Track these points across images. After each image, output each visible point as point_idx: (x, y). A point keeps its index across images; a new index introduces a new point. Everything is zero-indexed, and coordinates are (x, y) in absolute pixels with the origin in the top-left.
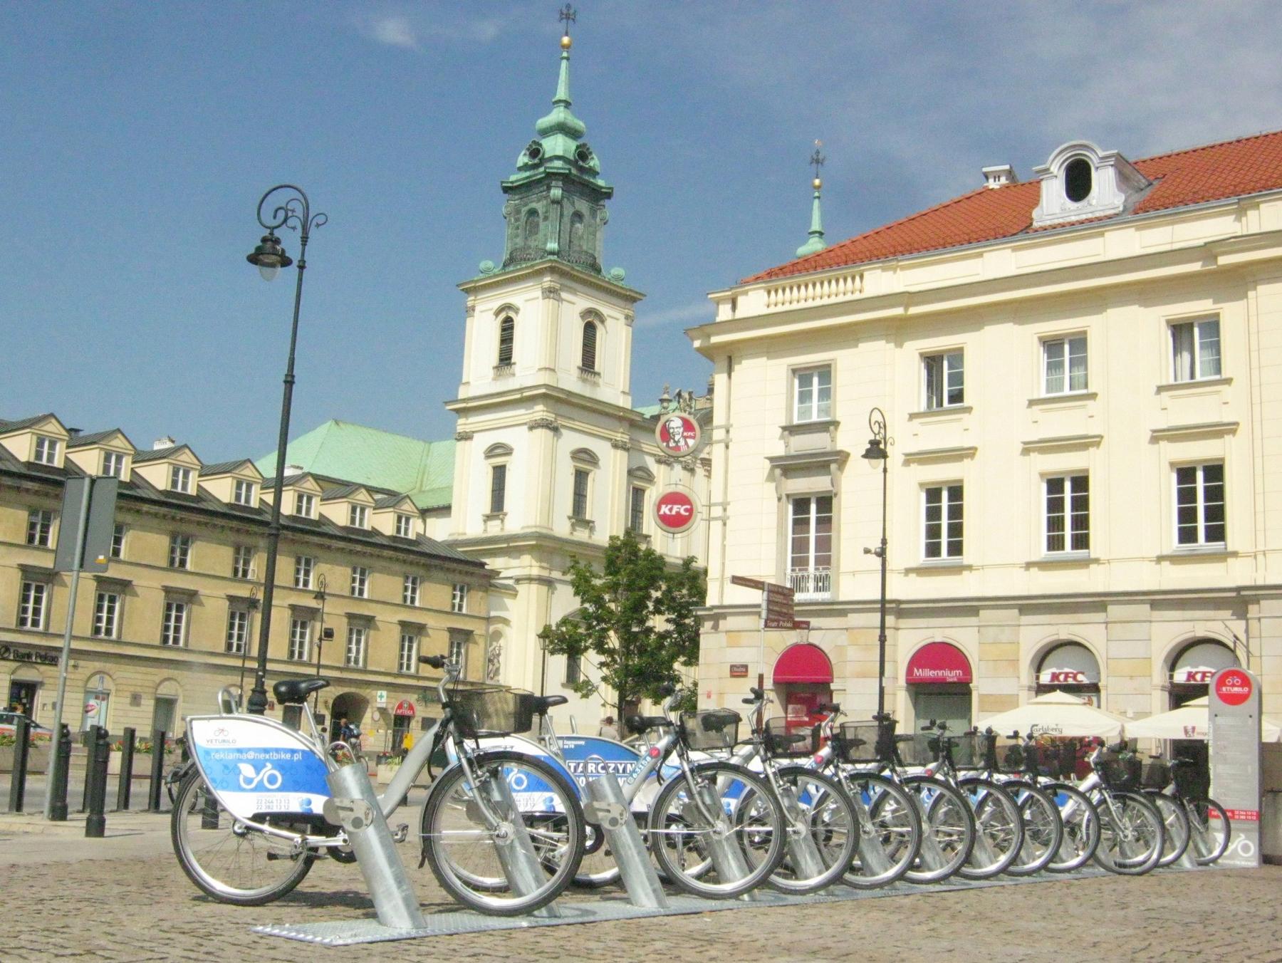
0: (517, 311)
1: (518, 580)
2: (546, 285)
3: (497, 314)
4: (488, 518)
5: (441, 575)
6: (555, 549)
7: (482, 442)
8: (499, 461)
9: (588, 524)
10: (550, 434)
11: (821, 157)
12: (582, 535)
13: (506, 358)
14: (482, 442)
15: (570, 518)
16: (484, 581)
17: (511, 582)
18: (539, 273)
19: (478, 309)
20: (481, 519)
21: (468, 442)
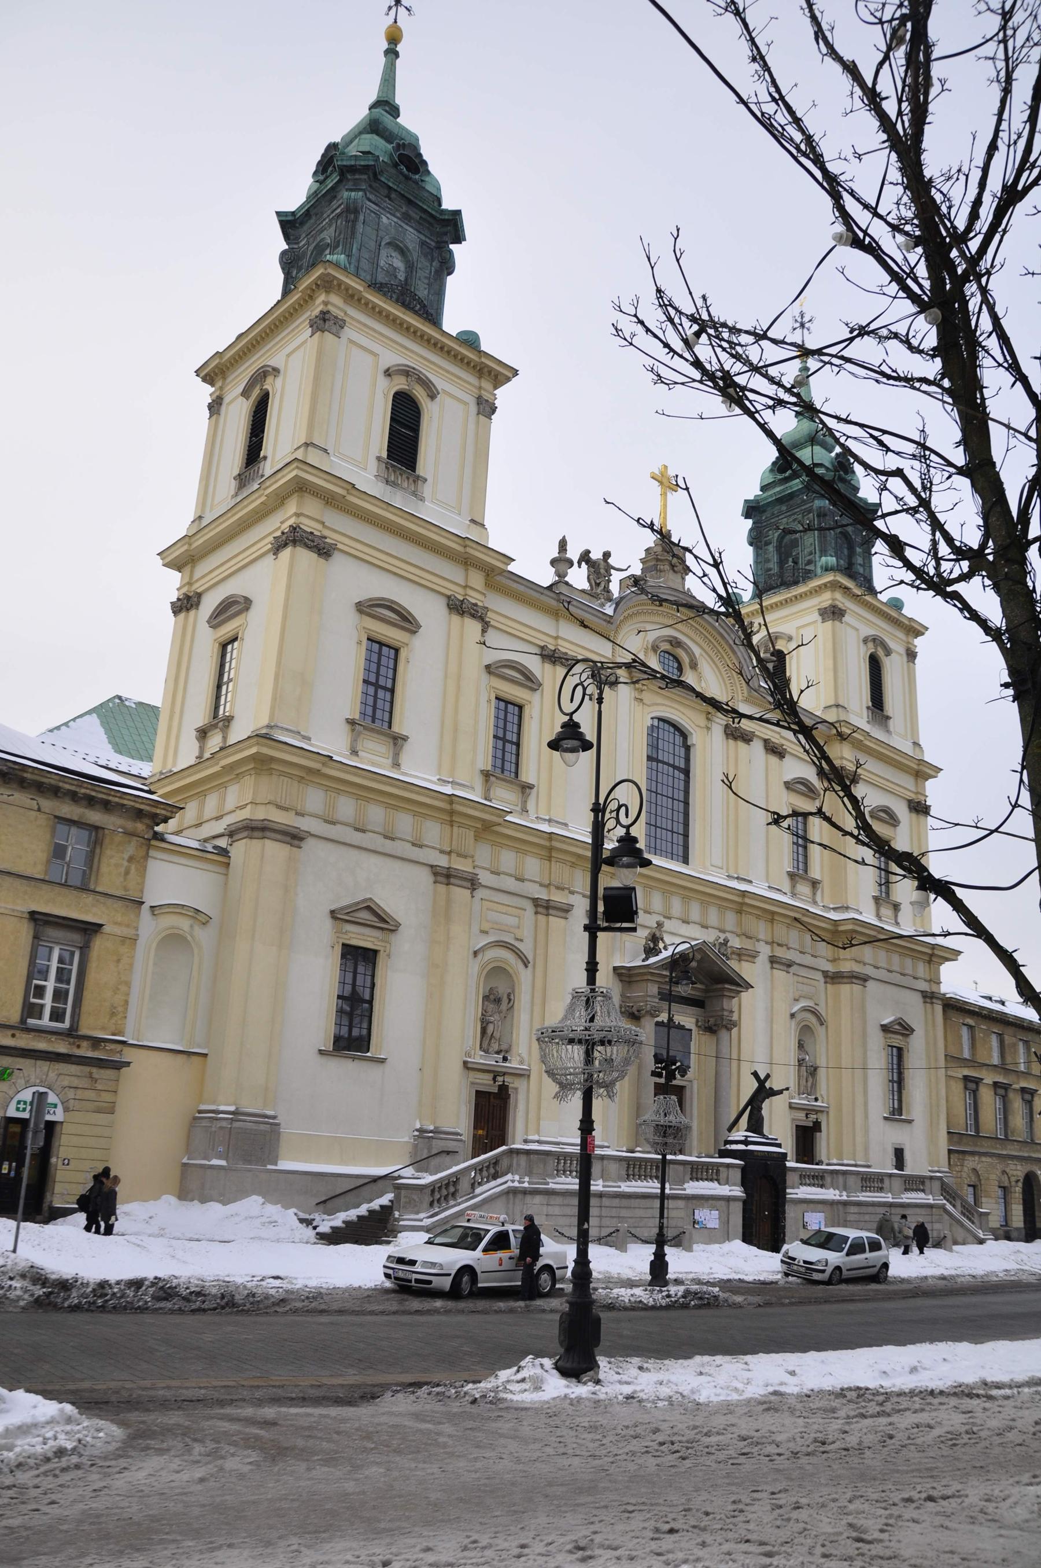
0: (276, 371)
1: (231, 833)
2: (317, 312)
3: (245, 393)
4: (203, 734)
5: (20, 797)
6: (310, 771)
7: (209, 604)
8: (227, 630)
9: (398, 741)
10: (305, 557)
11: (806, 319)
12: (373, 757)
13: (253, 454)
14: (209, 604)
15: (351, 722)
16: (140, 827)
17: (222, 843)
18: (309, 297)
19: (226, 400)
20: (194, 734)
21: (192, 613)
